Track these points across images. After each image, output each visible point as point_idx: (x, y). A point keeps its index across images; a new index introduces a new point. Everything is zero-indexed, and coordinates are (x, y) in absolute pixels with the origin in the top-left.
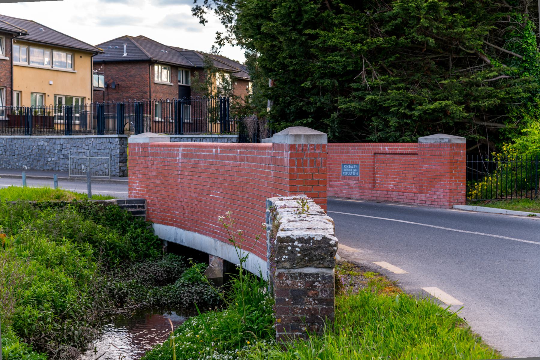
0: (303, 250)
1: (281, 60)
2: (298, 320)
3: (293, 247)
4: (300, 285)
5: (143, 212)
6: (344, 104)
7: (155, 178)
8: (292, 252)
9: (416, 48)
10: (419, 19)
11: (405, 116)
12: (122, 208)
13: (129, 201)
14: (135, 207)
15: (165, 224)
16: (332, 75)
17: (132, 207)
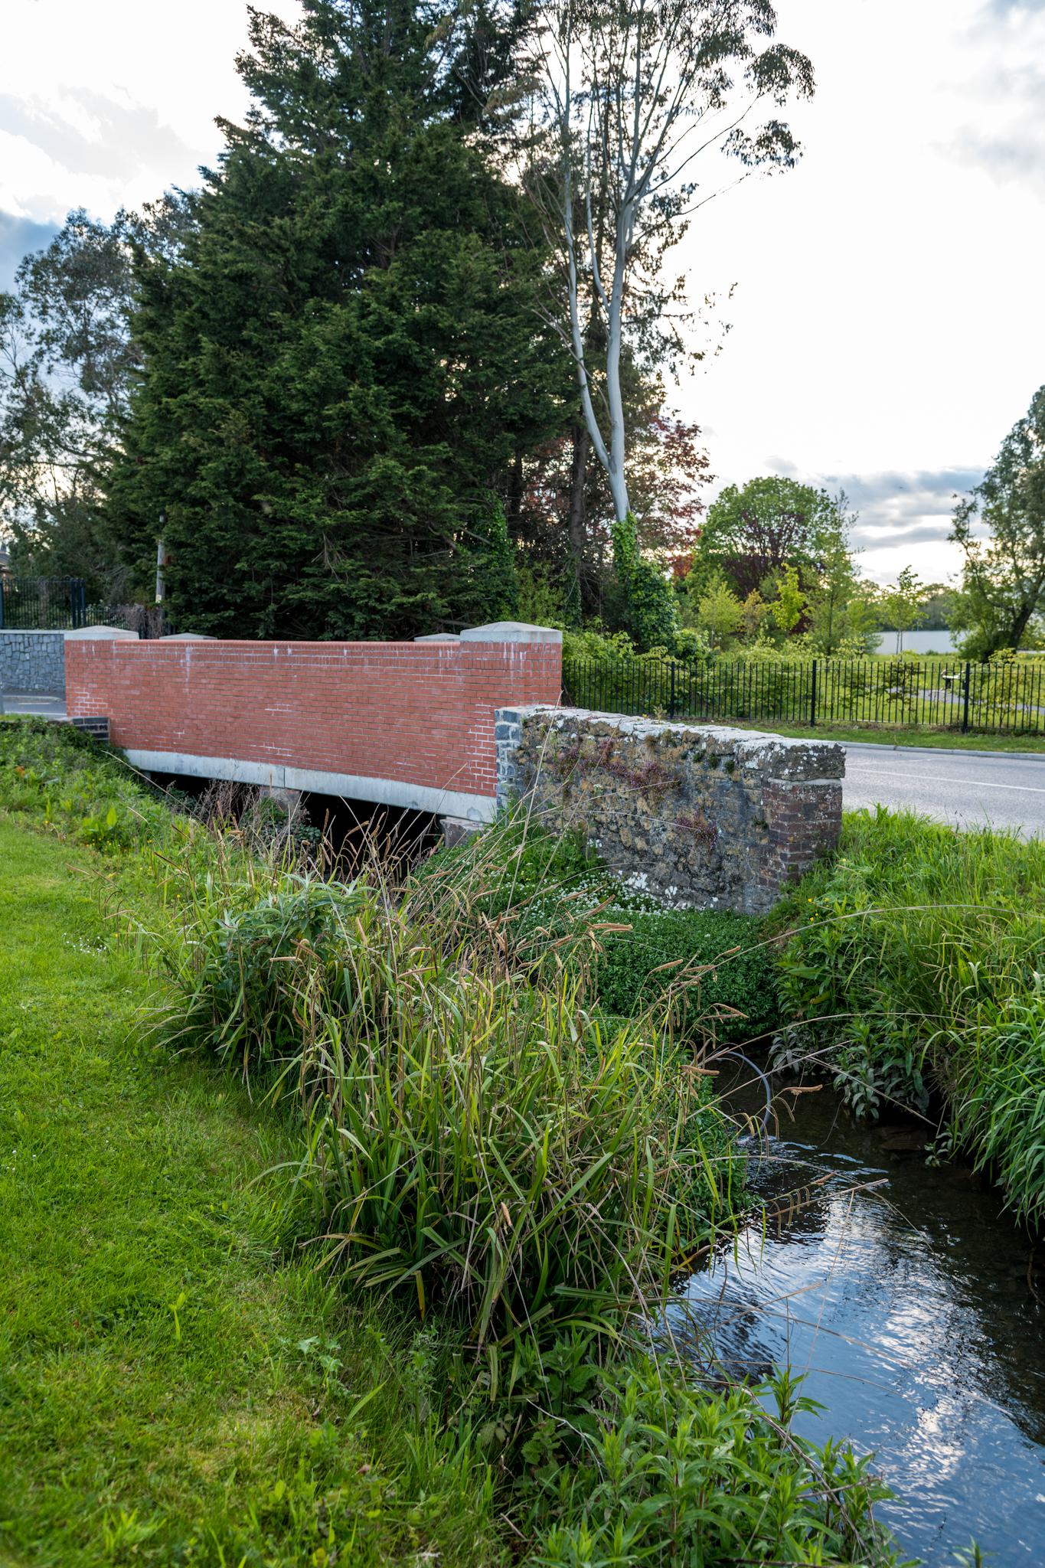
0: (820, 760)
1: (207, 532)
2: (808, 837)
3: (809, 757)
4: (813, 799)
5: (105, 735)
6: (294, 593)
7: (128, 688)
8: (808, 762)
9: (388, 524)
10: (402, 491)
11: (374, 610)
12: (81, 729)
13: (88, 721)
14: (95, 728)
15: (153, 750)
16: (281, 556)
17: (92, 728)
